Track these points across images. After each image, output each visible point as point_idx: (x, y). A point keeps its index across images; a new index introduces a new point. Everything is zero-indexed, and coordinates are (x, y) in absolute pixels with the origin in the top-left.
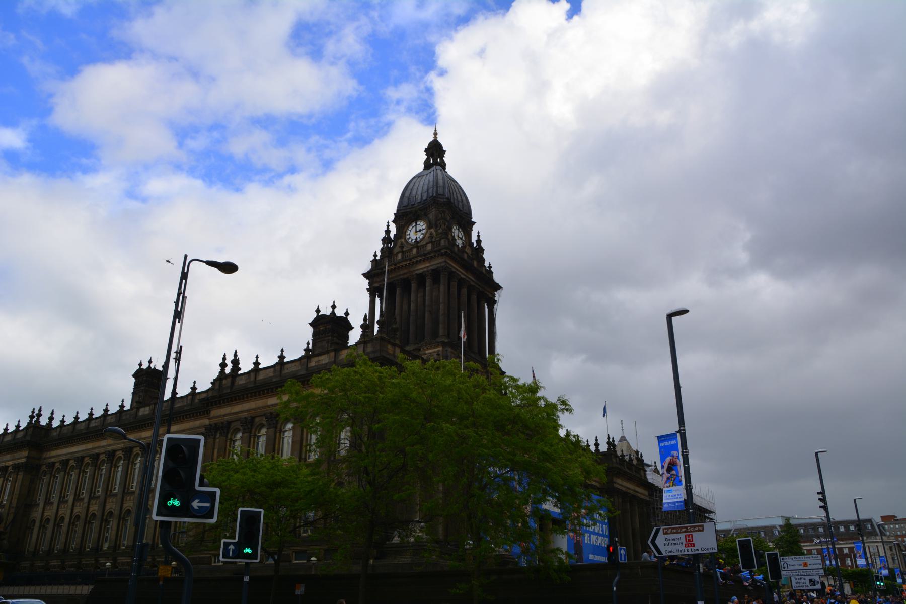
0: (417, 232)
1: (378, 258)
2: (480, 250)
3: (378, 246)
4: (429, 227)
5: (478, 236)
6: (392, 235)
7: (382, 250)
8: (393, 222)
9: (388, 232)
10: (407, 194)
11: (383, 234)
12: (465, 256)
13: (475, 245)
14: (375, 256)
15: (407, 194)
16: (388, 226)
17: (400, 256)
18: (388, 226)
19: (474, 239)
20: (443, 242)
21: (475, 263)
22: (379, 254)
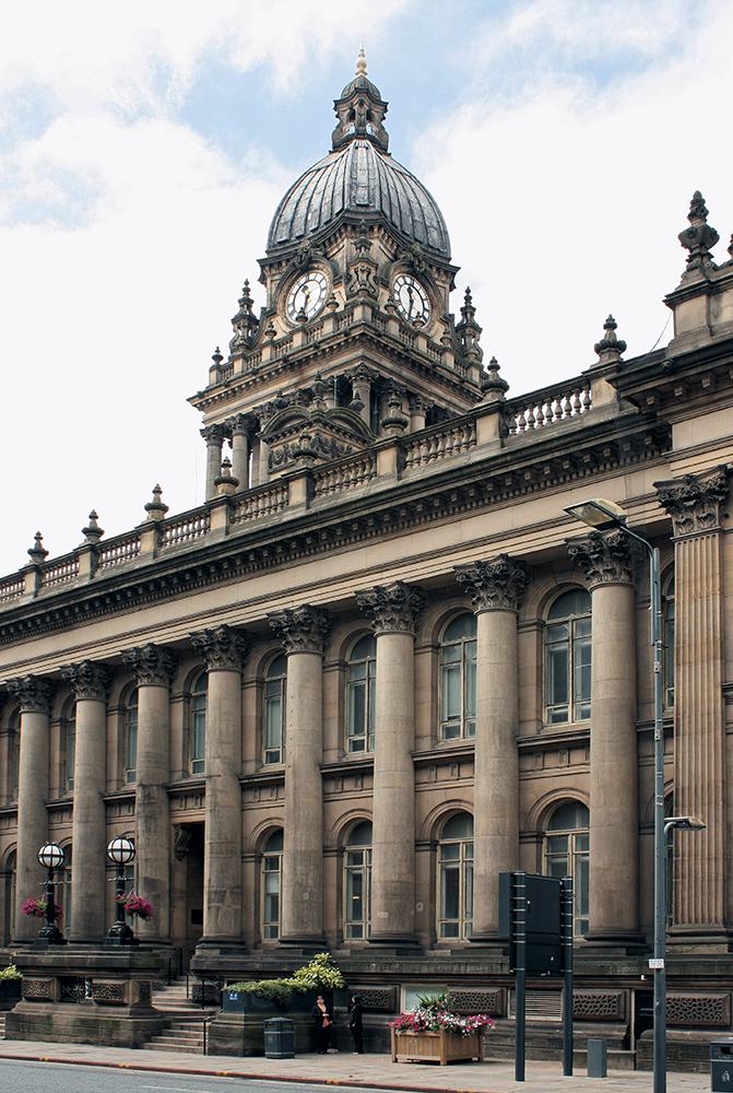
0: (313, 293)
1: (222, 363)
2: (469, 328)
3: (223, 336)
4: (336, 283)
5: (468, 299)
6: (256, 312)
7: (233, 343)
8: (263, 280)
9: (247, 302)
10: (288, 213)
11: (236, 310)
12: (422, 344)
13: (458, 319)
14: (218, 358)
15: (288, 213)
16: (247, 291)
17: (266, 354)
18: (247, 291)
19: (455, 303)
20: (358, 313)
21: (449, 360)
22: (226, 353)
